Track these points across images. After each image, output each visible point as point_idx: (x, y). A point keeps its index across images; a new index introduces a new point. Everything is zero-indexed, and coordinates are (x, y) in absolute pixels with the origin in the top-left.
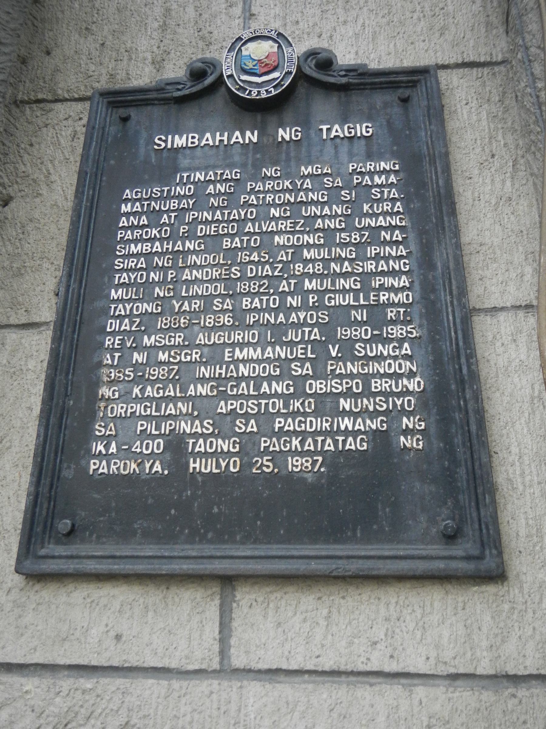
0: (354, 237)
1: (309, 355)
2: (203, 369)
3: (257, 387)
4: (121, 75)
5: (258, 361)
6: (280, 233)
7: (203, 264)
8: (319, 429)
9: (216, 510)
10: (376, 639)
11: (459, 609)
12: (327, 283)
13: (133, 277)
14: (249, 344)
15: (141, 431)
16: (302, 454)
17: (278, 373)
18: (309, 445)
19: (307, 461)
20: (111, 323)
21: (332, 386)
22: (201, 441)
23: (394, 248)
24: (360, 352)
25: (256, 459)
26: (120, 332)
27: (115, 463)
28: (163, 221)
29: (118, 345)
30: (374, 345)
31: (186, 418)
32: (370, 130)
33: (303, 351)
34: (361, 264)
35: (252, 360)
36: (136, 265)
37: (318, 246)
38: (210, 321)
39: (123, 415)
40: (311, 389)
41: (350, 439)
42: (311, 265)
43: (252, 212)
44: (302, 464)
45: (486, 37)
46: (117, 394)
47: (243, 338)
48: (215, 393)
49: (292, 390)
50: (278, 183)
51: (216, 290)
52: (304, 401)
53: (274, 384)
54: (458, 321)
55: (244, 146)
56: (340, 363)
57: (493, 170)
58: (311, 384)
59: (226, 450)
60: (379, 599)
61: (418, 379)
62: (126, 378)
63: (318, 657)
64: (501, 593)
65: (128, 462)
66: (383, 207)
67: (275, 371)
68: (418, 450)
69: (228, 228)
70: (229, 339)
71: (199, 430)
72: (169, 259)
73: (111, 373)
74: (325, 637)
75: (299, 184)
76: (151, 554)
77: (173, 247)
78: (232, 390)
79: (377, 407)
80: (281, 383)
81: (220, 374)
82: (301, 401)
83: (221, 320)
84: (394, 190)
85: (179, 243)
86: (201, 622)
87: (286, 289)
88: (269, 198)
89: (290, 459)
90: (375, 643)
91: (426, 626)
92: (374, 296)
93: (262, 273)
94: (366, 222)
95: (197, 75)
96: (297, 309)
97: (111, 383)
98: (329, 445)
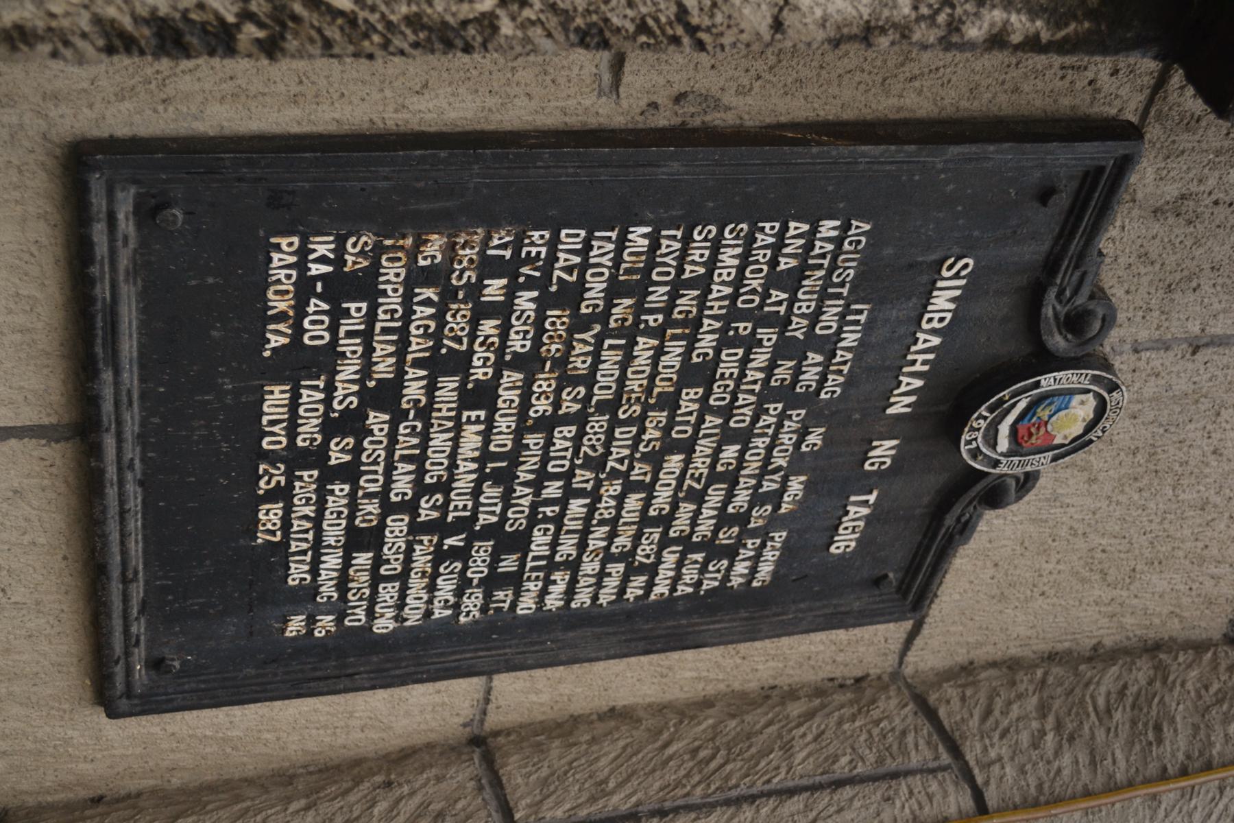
5: (453, 456)
10: (9, 593)
15: (348, 309)
22: (321, 396)
25: (282, 467)
29: (529, 253)
47: (500, 433)
83: (543, 401)
91: (34, 639)
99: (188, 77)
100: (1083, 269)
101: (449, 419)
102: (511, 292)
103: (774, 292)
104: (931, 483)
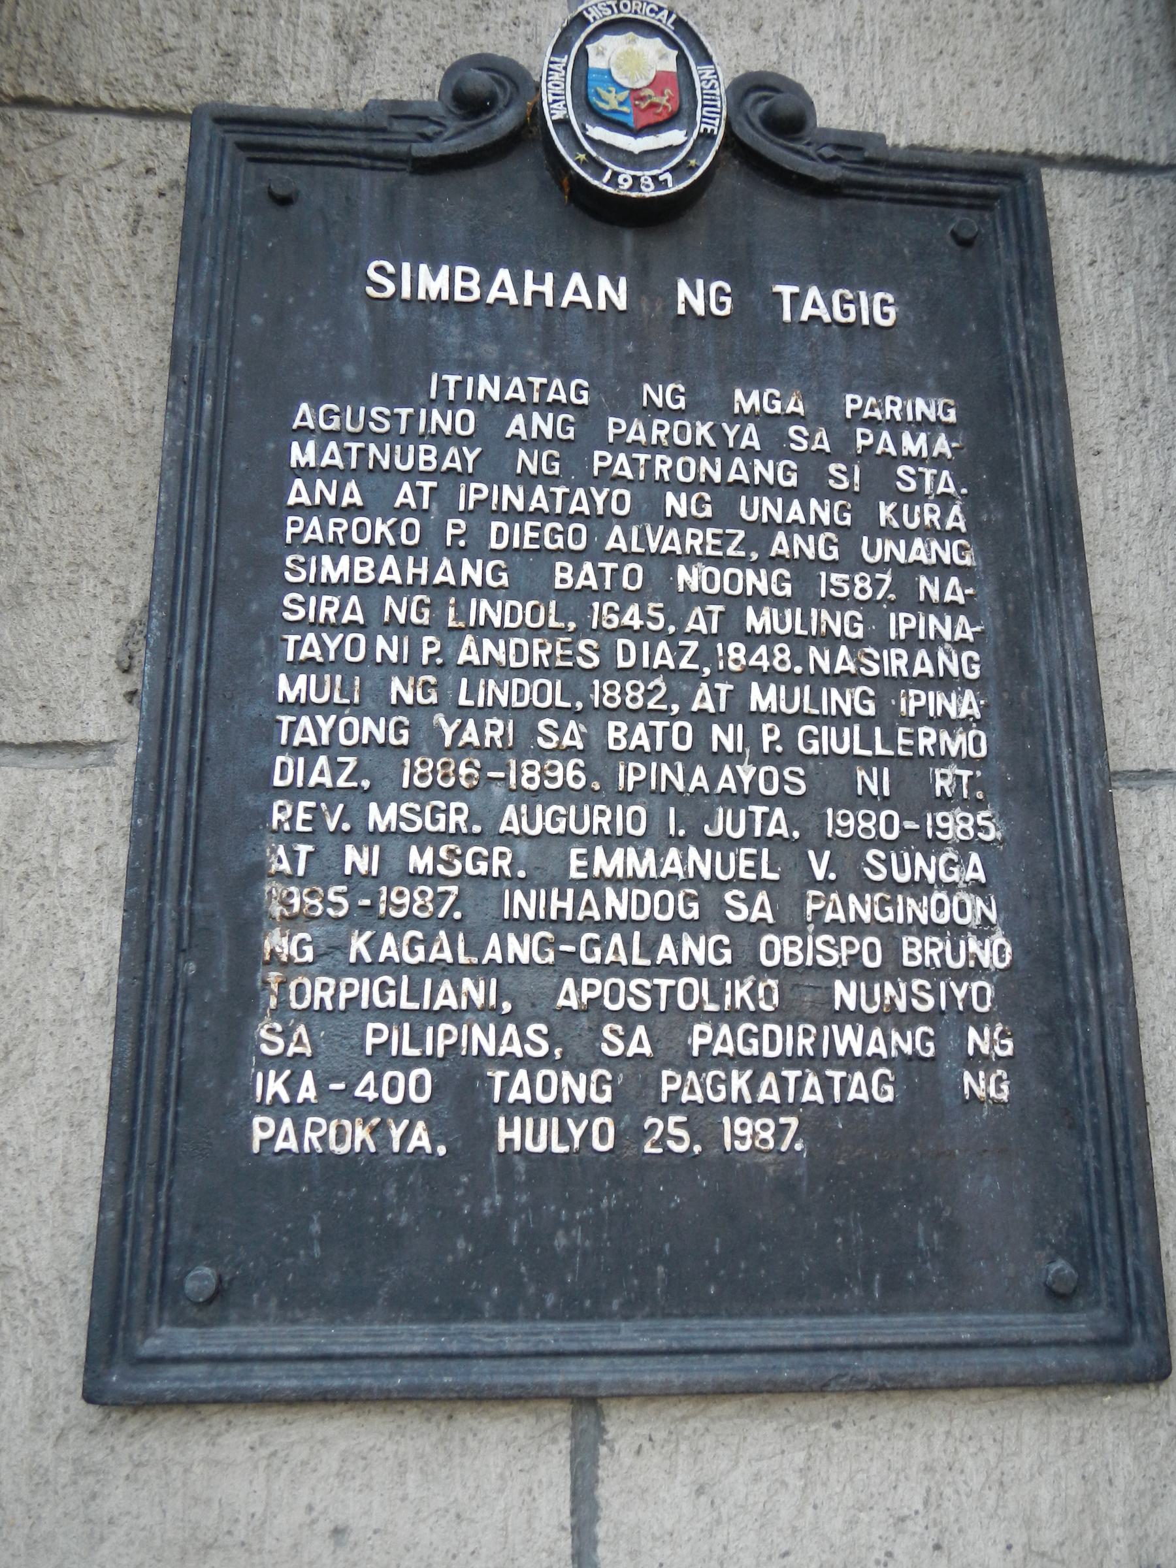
0: (859, 585)
1: (766, 874)
2: (519, 896)
4: (253, 59)
5: (650, 883)
6: (690, 559)
7: (507, 624)
8: (789, 1053)
9: (561, 1241)
10: (906, 1511)
11: (1073, 1442)
12: (802, 698)
13: (332, 646)
14: (626, 840)
15: (374, 1046)
16: (755, 1110)
17: (695, 914)
18: (769, 1090)
19: (765, 1127)
20: (284, 765)
21: (816, 951)
22: (522, 1075)
23: (948, 619)
24: (875, 870)
25: (650, 1121)
26: (306, 791)
27: (315, 1127)
28: (400, 500)
31: (483, 1016)
32: (891, 311)
33: (751, 864)
34: (876, 656)
35: (635, 881)
36: (339, 614)
37: (781, 603)
38: (530, 776)
39: (329, 1007)
40: (770, 956)
41: (858, 1076)
42: (763, 650)
43: (621, 498)
44: (755, 1134)
45: (1134, 95)
46: (309, 950)
47: (612, 823)
48: (550, 959)
49: (727, 957)
50: (682, 428)
51: (542, 698)
52: (755, 984)
53: (687, 942)
54: (1084, 809)
55: (593, 314)
56: (834, 896)
57: (1145, 436)
58: (770, 944)
59: (581, 1098)
60: (911, 1426)
61: (999, 939)
62: (331, 912)
63: (786, 1554)
64: (1154, 1408)
65: (347, 1123)
66: (921, 515)
67: (688, 909)
68: (1000, 1102)
69: (564, 533)
70: (579, 823)
71: (517, 1050)
72: (421, 603)
73: (290, 895)
74: (800, 1512)
75: (731, 435)
76: (416, 1348)
78: (590, 953)
79: (915, 1002)
80: (702, 939)
83: (559, 773)
85: (446, 563)
86: (530, 1491)
87: (709, 706)
89: (726, 1120)
90: (903, 1519)
91: (1006, 1479)
92: (905, 735)
93: (651, 658)
94: (887, 548)
95: (469, 104)
96: (736, 758)
97: (292, 921)
98: (813, 1091)
99: (32, 1256)
100: (385, 124)
101: (578, 898)
102: (367, 837)
103: (400, 500)
104: (775, 213)
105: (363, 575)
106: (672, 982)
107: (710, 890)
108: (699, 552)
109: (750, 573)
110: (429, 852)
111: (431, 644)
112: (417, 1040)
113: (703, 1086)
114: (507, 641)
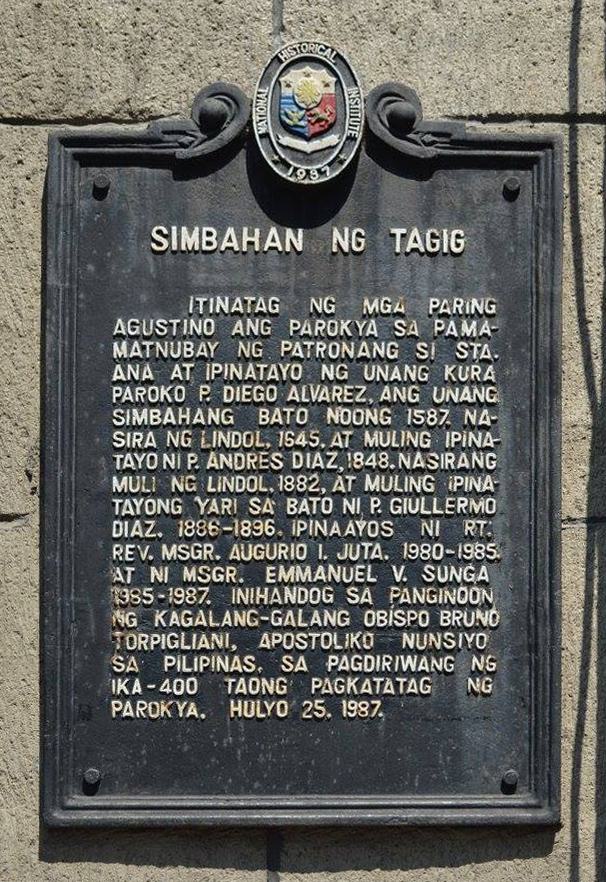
0: (430, 416)
1: (370, 579)
3: (307, 617)
4: (77, 80)
5: (308, 585)
6: (335, 404)
7: (234, 446)
8: (378, 670)
9: (261, 759)
12: (394, 483)
13: (140, 460)
15: (169, 668)
16: (358, 697)
17: (331, 600)
18: (367, 687)
19: (364, 706)
20: (118, 526)
21: (394, 618)
22: (242, 680)
24: (429, 577)
25: (306, 702)
27: (142, 705)
28: (174, 375)
29: (130, 556)
30: (446, 568)
33: (362, 574)
34: (437, 458)
36: (143, 442)
38: (245, 528)
41: (413, 681)
42: (373, 456)
43: (297, 369)
46: (135, 621)
47: (288, 554)
48: (256, 623)
49: (348, 621)
51: (252, 486)
53: (327, 614)
56: (406, 590)
61: (493, 611)
62: (145, 602)
65: (156, 703)
66: (470, 373)
70: (271, 554)
73: (124, 593)
77: (192, 418)
80: (335, 612)
81: (262, 600)
82: (358, 635)
84: (486, 346)
87: (342, 489)
88: (320, 348)
92: (450, 503)
94: (448, 393)
95: (210, 123)
101: (270, 592)
103: (174, 375)
105: (155, 420)
106: (318, 635)
107: (339, 589)
108: (340, 400)
109: (368, 411)
110: (193, 571)
111: (192, 458)
112: (190, 664)
113: (333, 686)
114: (233, 453)
